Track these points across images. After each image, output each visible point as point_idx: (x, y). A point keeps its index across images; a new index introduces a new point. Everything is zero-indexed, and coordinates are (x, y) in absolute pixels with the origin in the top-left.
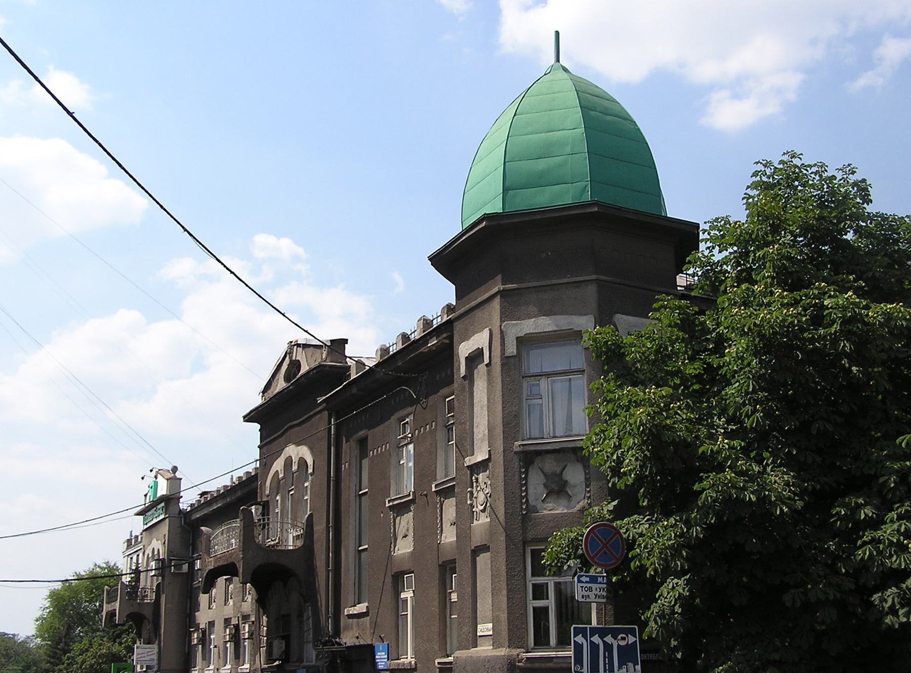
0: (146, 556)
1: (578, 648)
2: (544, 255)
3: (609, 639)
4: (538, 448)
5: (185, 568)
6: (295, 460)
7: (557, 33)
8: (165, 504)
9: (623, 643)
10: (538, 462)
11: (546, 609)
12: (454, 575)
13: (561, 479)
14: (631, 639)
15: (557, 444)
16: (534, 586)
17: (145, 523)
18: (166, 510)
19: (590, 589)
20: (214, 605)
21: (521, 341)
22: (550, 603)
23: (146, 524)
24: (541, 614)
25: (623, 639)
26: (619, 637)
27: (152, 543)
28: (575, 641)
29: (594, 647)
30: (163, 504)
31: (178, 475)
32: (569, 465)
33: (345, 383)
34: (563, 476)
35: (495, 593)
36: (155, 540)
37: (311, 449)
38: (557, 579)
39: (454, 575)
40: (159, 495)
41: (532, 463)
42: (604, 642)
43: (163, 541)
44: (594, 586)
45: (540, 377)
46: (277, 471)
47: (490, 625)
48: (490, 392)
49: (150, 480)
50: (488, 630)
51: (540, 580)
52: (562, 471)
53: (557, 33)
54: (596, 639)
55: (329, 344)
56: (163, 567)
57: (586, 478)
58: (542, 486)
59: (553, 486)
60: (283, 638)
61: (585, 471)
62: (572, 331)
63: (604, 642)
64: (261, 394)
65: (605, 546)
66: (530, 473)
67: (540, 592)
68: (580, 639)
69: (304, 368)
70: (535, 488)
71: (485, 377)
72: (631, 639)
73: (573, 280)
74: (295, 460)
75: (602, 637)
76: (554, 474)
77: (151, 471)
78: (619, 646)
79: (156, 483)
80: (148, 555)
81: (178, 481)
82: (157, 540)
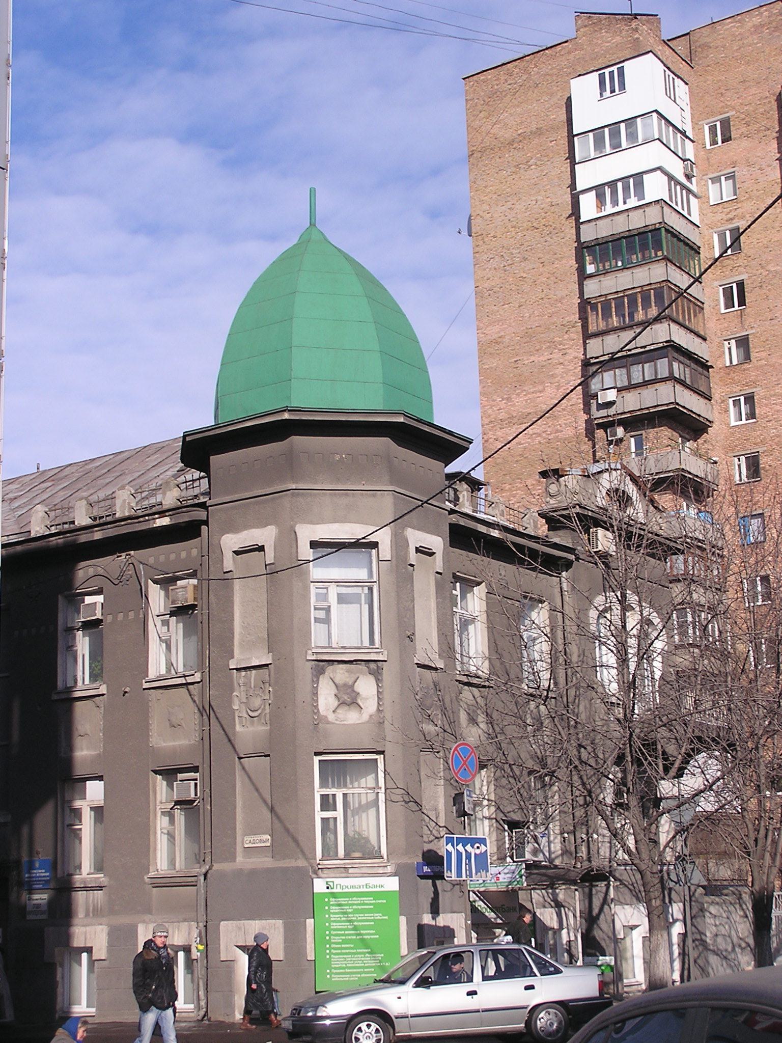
2: (337, 457)
3: (468, 847)
9: (478, 852)
10: (330, 670)
12: (175, 783)
13: (354, 691)
14: (483, 848)
15: (353, 655)
21: (314, 545)
25: (478, 848)
29: (459, 854)
32: (361, 677)
38: (345, 791)
39: (175, 783)
41: (321, 672)
42: (466, 850)
51: (326, 791)
52: (355, 682)
54: (460, 847)
57: (378, 692)
58: (334, 697)
59: (346, 698)
61: (378, 685)
63: (466, 850)
65: (465, 762)
66: (320, 682)
68: (450, 847)
70: (326, 699)
72: (483, 848)
75: (464, 846)
76: (345, 685)
78: (475, 854)
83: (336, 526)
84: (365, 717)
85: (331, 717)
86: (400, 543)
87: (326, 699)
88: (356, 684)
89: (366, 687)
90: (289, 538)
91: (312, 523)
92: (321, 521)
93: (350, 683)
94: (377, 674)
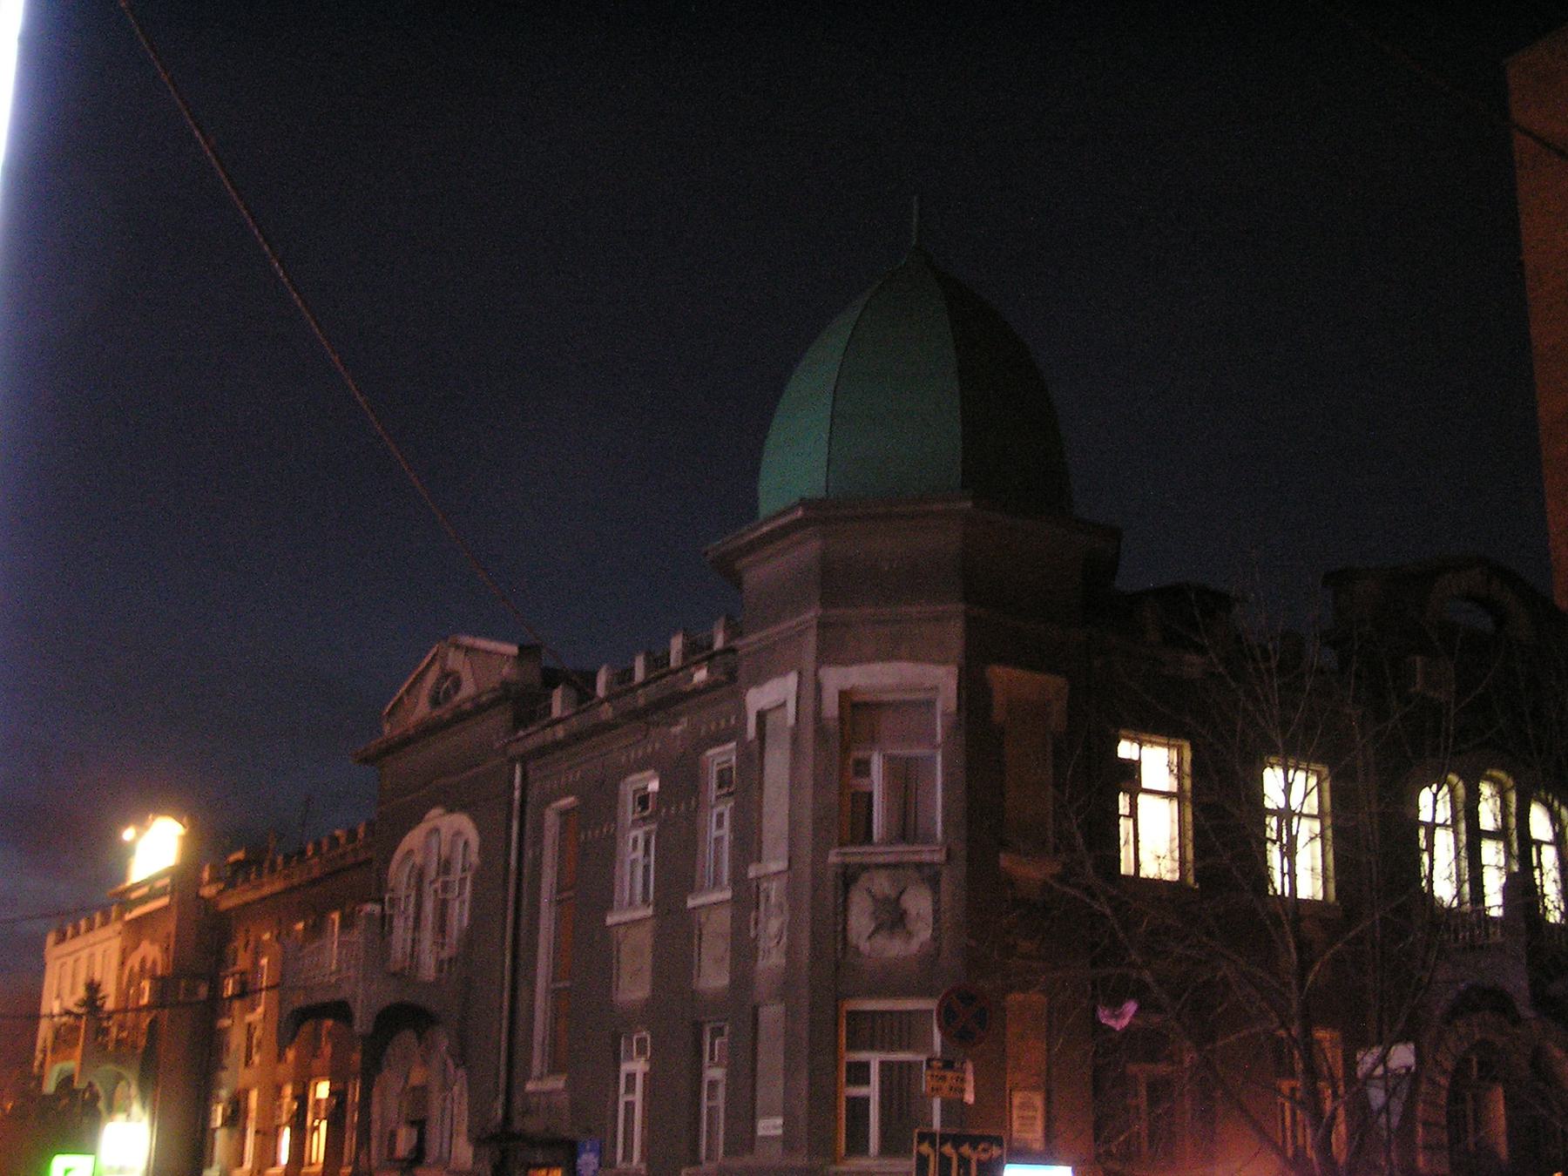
0: (127, 972)
1: (923, 1161)
3: (966, 1149)
4: (866, 860)
5: (203, 991)
6: (446, 833)
9: (984, 1156)
10: (864, 879)
11: (866, 1100)
16: (850, 1065)
19: (944, 1078)
20: (256, 1059)
22: (873, 1091)
24: (858, 1108)
25: (985, 1150)
26: (980, 1147)
28: (918, 1152)
29: (945, 1162)
34: (901, 902)
35: (789, 1073)
37: (474, 819)
44: (949, 1074)
47: (779, 1121)
48: (794, 769)
50: (775, 1128)
54: (948, 1149)
56: (164, 986)
60: (413, 1123)
67: (859, 1073)
68: (925, 1148)
69: (468, 689)
71: (787, 746)
74: (446, 833)
75: (956, 1147)
76: (887, 899)
78: (978, 1160)
80: (131, 970)
83: (877, 667)
84: (915, 945)
85: (865, 946)
86: (973, 692)
87: (860, 921)
88: (903, 897)
89: (919, 903)
92: (858, 660)
93: (893, 895)
94: (934, 883)
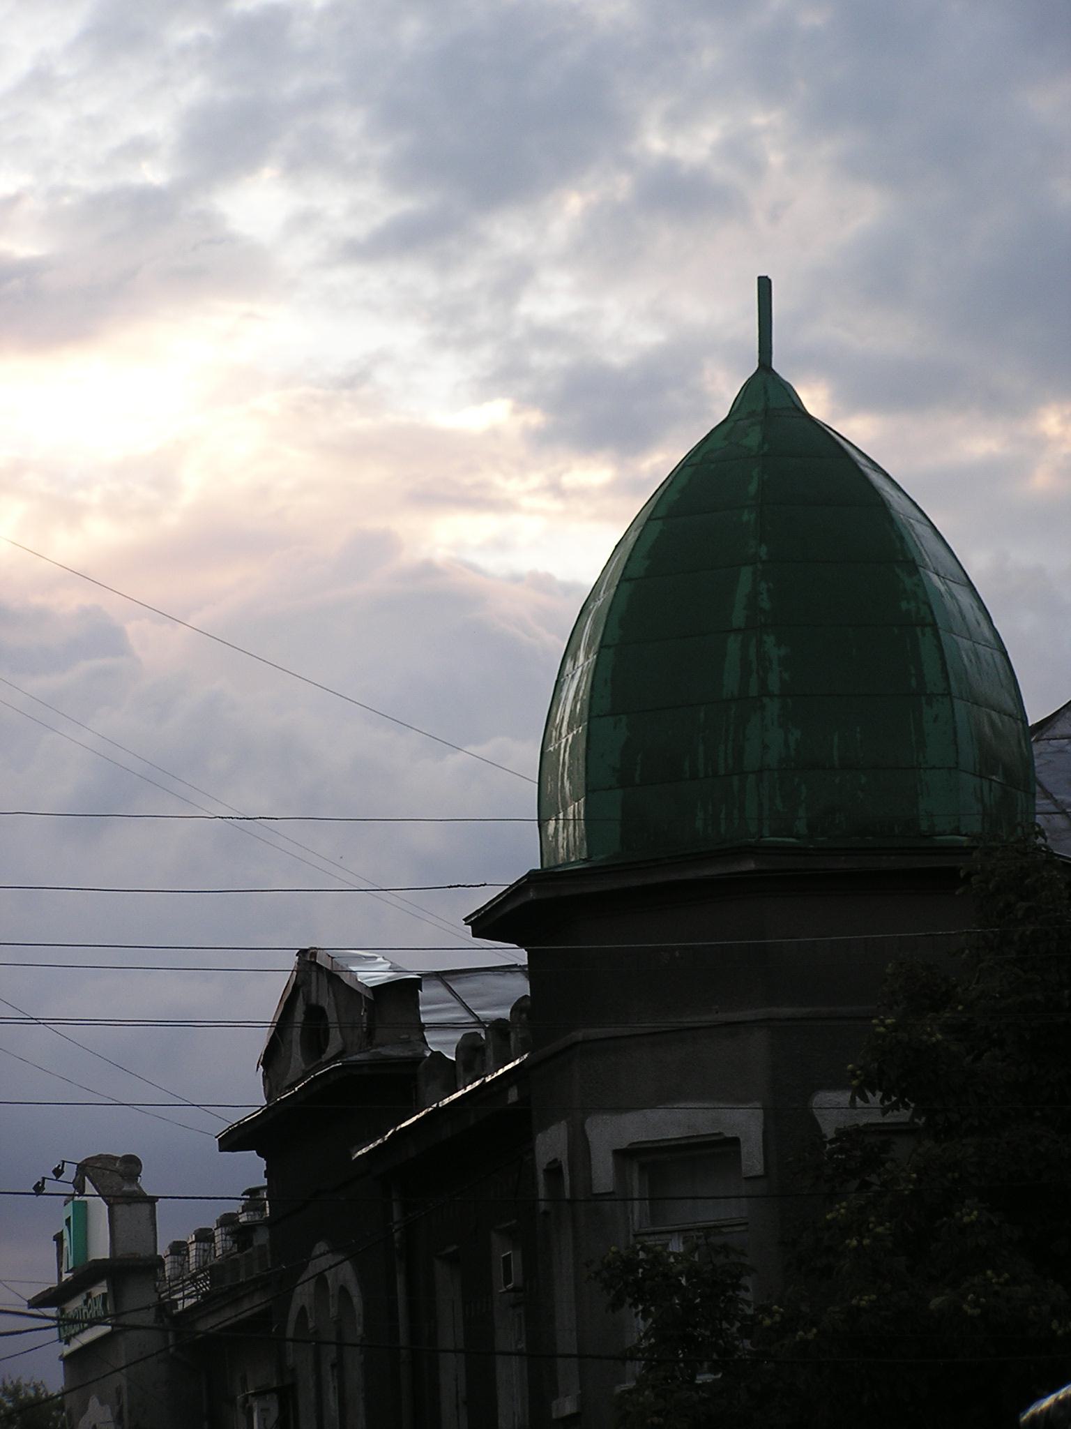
7: (765, 285)
8: (112, 1286)
17: (64, 1335)
18: (116, 1305)
23: (67, 1342)
27: (89, 1409)
30: (100, 1289)
31: (148, 1183)
33: (364, 1151)
36: (94, 1402)
40: (90, 1260)
43: (117, 1408)
45: (669, 1236)
46: (303, 1308)
49: (56, 1213)
53: (765, 285)
55: (369, 996)
62: (721, 1137)
64: (261, 1067)
73: (723, 1017)
77: (58, 1172)
79: (82, 1212)
81: (145, 1208)
82: (102, 1403)
90: (580, 1146)
91: (619, 1109)
